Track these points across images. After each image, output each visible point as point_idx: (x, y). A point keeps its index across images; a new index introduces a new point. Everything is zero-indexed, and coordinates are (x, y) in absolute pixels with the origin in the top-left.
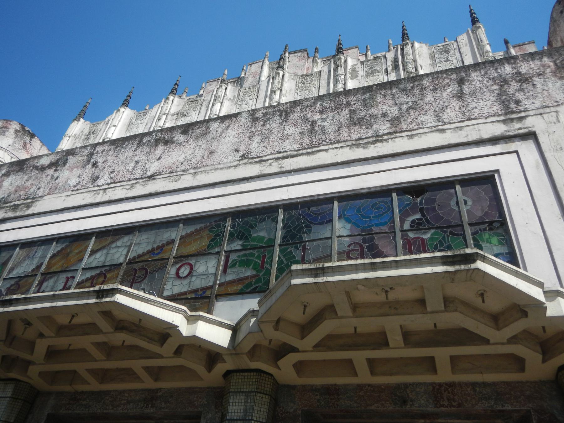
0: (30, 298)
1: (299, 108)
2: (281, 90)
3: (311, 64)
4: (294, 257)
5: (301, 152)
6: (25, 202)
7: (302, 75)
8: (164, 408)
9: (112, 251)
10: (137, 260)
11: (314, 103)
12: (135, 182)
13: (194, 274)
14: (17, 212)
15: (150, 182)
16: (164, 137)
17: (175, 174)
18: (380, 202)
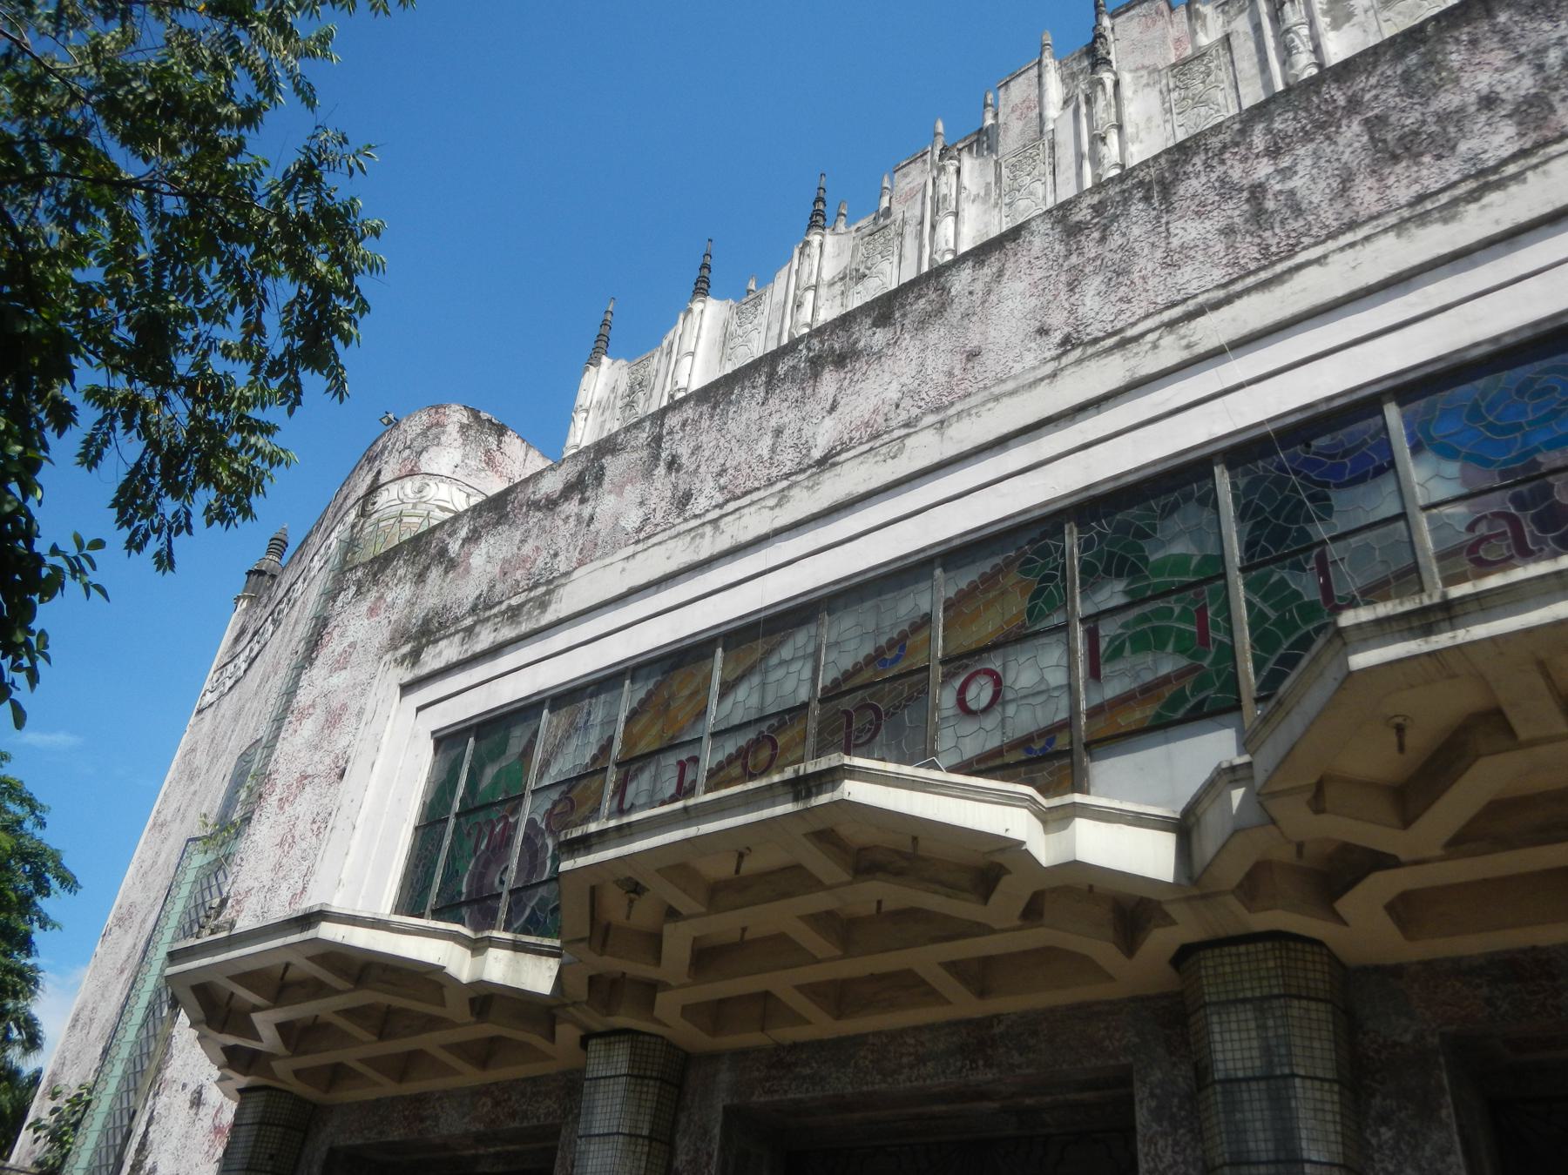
0: (629, 824)
1: (1198, 161)
2: (1120, 128)
3: (1186, 27)
4: (1297, 595)
5: (1238, 287)
6: (532, 594)
7: (1174, 66)
8: (1019, 1066)
9: (775, 676)
11: (1242, 132)
12: (785, 483)
13: (1010, 695)
14: (519, 623)
15: (827, 475)
16: (832, 348)
17: (886, 438)
18: (1546, 372)
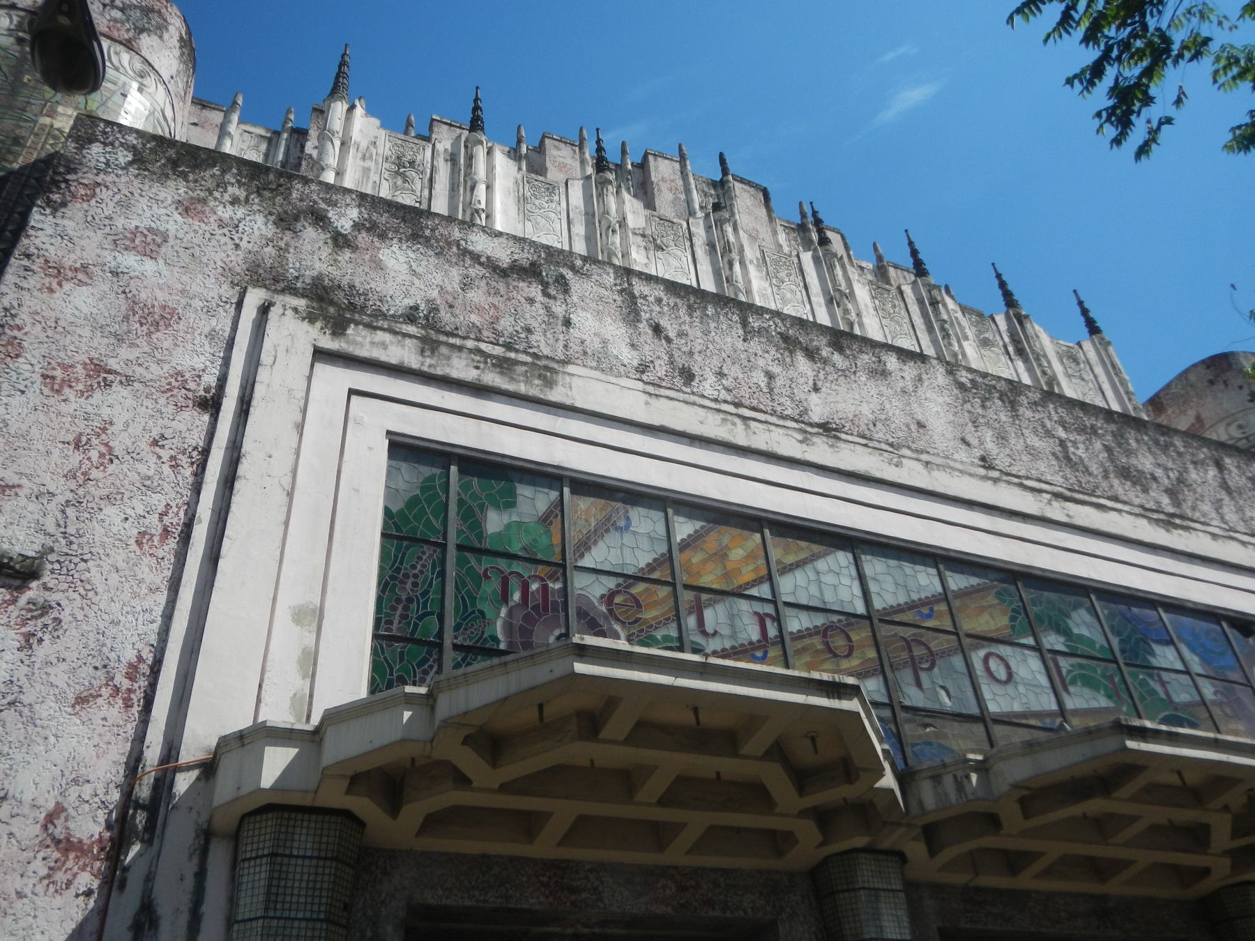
0: (1177, 734)
6: (512, 355)
10: (897, 618)
